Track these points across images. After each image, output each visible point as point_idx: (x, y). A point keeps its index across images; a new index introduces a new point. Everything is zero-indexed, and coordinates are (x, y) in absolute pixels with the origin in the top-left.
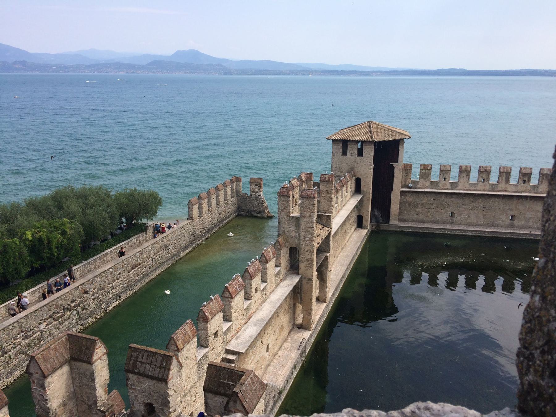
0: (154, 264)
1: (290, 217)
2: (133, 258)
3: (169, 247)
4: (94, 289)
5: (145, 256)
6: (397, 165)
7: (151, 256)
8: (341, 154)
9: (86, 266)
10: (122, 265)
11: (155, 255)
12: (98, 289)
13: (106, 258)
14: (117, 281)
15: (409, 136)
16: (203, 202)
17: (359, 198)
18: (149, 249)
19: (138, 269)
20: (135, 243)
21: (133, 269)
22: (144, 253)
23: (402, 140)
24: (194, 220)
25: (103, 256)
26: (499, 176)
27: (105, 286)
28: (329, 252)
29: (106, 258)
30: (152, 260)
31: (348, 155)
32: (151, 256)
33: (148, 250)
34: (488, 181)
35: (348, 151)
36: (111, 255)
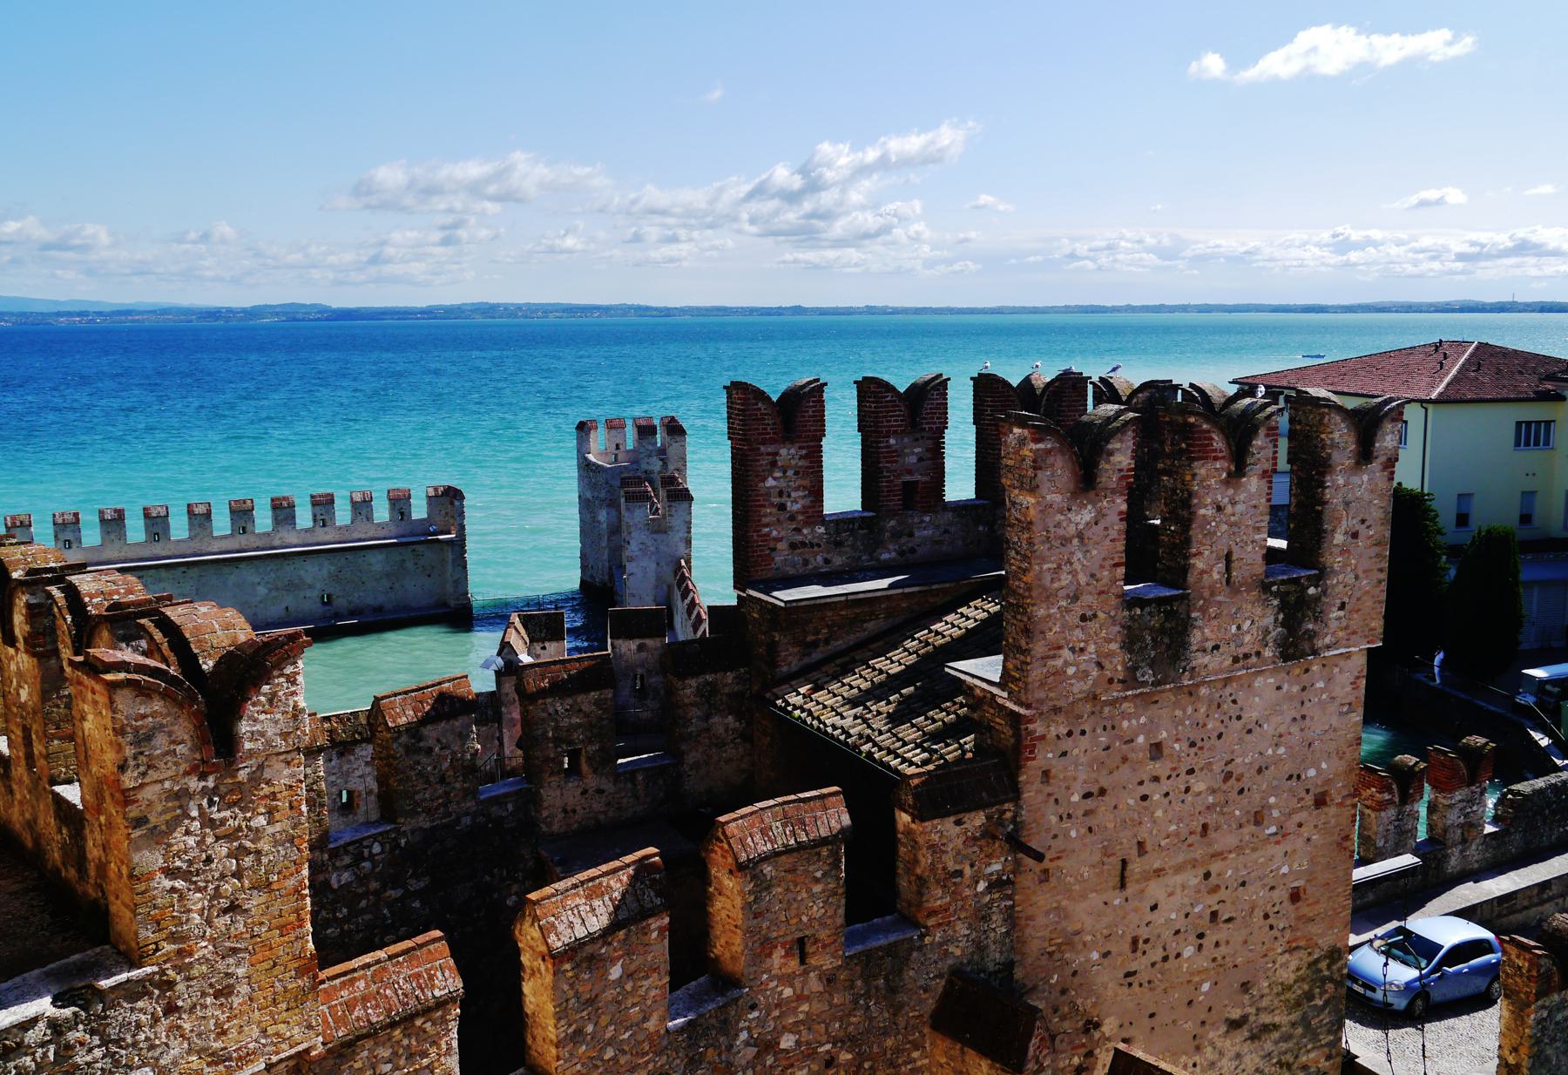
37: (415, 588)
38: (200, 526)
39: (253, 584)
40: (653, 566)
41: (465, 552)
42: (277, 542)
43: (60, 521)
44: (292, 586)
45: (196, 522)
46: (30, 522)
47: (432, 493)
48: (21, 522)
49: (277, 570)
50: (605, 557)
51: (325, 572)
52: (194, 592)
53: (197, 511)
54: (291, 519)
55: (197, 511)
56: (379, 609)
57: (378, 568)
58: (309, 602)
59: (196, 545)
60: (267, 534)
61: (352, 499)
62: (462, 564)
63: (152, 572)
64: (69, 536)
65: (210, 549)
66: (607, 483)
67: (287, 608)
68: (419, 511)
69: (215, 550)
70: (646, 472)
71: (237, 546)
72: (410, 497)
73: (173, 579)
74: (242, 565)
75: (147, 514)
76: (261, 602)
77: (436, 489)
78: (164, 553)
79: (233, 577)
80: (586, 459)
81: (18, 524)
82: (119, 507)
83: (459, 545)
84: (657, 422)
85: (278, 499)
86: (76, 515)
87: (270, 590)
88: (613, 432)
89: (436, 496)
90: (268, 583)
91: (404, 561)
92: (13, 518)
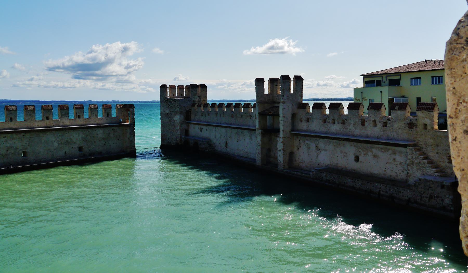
37: (113, 144)
40: (291, 105)
41: (134, 129)
42: (61, 124)
44: (68, 143)
47: (119, 107)
49: (62, 135)
50: (179, 132)
51: (80, 137)
52: (28, 145)
54: (67, 115)
56: (100, 153)
57: (100, 136)
58: (73, 150)
59: (28, 124)
61: (90, 107)
62: (133, 134)
63: (10, 135)
65: (34, 126)
66: (180, 105)
67: (65, 152)
68: (114, 114)
69: (36, 126)
70: (193, 101)
71: (45, 125)
72: (111, 108)
73: (19, 138)
74: (48, 133)
76: (55, 149)
77: (120, 105)
80: (166, 98)
83: (132, 126)
84: (185, 87)
85: (62, 105)
87: (59, 145)
88: (172, 89)
89: (121, 108)
90: (58, 141)
91: (110, 133)
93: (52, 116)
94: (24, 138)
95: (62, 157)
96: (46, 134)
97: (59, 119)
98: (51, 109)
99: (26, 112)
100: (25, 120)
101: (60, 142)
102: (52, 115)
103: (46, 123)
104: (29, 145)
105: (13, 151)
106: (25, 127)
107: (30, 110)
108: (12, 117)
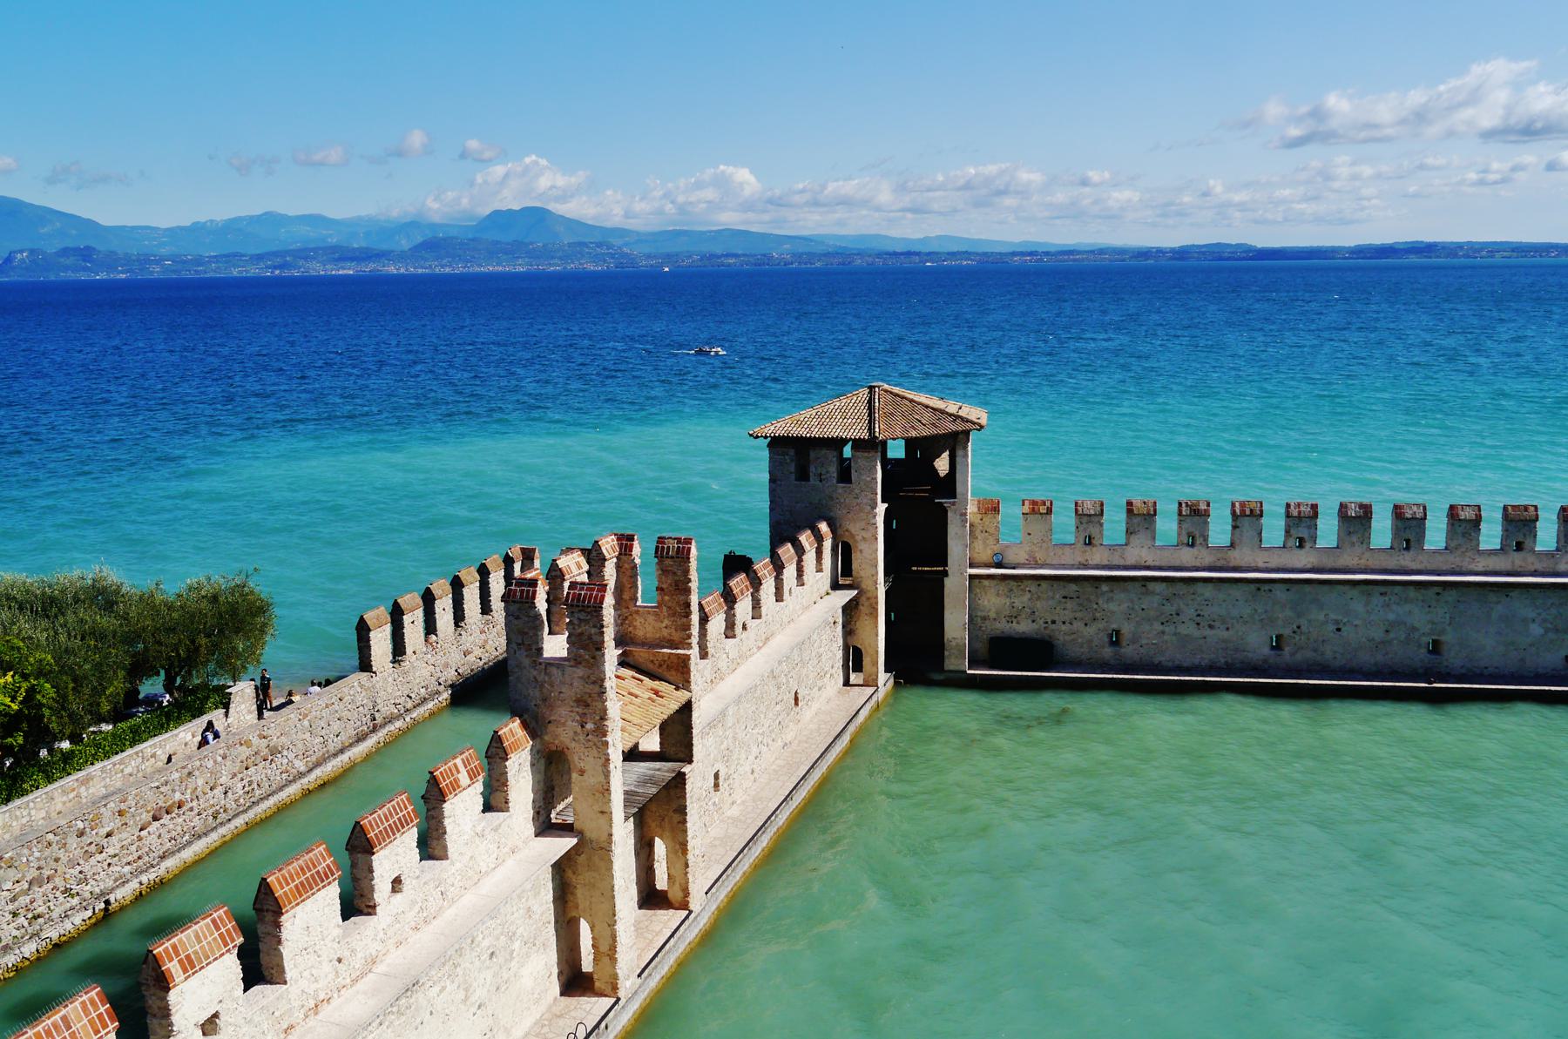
0: (231, 805)
1: (540, 664)
2: (158, 788)
3: (285, 753)
4: (18, 882)
5: (200, 782)
6: (954, 504)
7: (223, 780)
8: (793, 477)
9: (18, 813)
10: (117, 809)
11: (234, 775)
12: (31, 884)
13: (87, 789)
14: (99, 857)
15: (979, 424)
16: (407, 619)
17: (846, 596)
18: (215, 762)
19: (172, 818)
20: (186, 744)
21: (155, 819)
22: (197, 773)
23: (967, 433)
24: (375, 673)
25: (76, 784)
26: (1235, 527)
27: (56, 871)
28: (690, 761)
29: (87, 789)
30: (226, 793)
31: (813, 481)
32: (223, 780)
33: (210, 764)
34: (1206, 539)
35: (812, 469)
36: (104, 779)
38: (1464, 535)
39: (1525, 621)
43: (1295, 513)
45: (1460, 530)
46: (1261, 511)
48: (1251, 510)
52: (1448, 622)
53: (1462, 515)
55: (1462, 515)
59: (1453, 560)
60: (1549, 555)
63: (1397, 589)
64: (1304, 533)
65: (1473, 567)
69: (1480, 568)
74: (1515, 594)
75: (1398, 511)
78: (1414, 566)
79: (1500, 607)
81: (1248, 512)
82: (1365, 501)
86: (1314, 507)
87: (1547, 631)
90: (1544, 620)
92: (1243, 504)
93: (1535, 542)
94: (1438, 601)
95: (1553, 670)
96: (1507, 596)
97: (1558, 549)
98: (1534, 518)
99: (1453, 525)
100: (1446, 548)
101: (1551, 623)
102: (1535, 536)
103: (1513, 562)
104: (1450, 624)
105: (1403, 637)
106: (1444, 568)
107: (1465, 520)
108: (1411, 535)
